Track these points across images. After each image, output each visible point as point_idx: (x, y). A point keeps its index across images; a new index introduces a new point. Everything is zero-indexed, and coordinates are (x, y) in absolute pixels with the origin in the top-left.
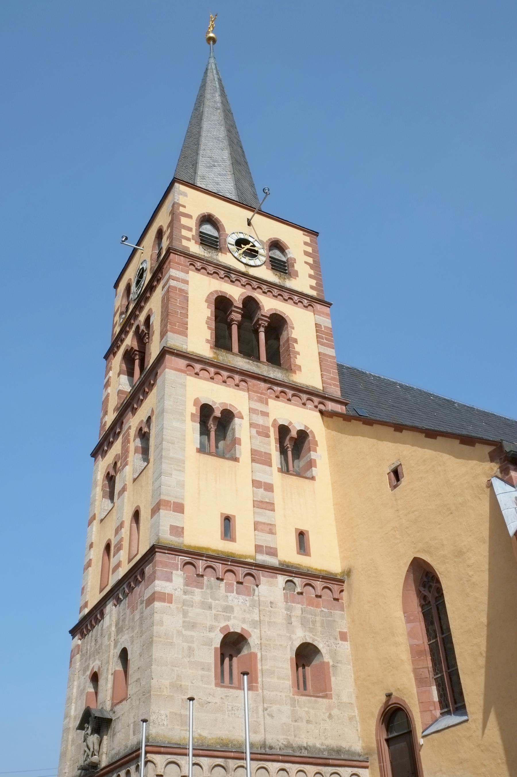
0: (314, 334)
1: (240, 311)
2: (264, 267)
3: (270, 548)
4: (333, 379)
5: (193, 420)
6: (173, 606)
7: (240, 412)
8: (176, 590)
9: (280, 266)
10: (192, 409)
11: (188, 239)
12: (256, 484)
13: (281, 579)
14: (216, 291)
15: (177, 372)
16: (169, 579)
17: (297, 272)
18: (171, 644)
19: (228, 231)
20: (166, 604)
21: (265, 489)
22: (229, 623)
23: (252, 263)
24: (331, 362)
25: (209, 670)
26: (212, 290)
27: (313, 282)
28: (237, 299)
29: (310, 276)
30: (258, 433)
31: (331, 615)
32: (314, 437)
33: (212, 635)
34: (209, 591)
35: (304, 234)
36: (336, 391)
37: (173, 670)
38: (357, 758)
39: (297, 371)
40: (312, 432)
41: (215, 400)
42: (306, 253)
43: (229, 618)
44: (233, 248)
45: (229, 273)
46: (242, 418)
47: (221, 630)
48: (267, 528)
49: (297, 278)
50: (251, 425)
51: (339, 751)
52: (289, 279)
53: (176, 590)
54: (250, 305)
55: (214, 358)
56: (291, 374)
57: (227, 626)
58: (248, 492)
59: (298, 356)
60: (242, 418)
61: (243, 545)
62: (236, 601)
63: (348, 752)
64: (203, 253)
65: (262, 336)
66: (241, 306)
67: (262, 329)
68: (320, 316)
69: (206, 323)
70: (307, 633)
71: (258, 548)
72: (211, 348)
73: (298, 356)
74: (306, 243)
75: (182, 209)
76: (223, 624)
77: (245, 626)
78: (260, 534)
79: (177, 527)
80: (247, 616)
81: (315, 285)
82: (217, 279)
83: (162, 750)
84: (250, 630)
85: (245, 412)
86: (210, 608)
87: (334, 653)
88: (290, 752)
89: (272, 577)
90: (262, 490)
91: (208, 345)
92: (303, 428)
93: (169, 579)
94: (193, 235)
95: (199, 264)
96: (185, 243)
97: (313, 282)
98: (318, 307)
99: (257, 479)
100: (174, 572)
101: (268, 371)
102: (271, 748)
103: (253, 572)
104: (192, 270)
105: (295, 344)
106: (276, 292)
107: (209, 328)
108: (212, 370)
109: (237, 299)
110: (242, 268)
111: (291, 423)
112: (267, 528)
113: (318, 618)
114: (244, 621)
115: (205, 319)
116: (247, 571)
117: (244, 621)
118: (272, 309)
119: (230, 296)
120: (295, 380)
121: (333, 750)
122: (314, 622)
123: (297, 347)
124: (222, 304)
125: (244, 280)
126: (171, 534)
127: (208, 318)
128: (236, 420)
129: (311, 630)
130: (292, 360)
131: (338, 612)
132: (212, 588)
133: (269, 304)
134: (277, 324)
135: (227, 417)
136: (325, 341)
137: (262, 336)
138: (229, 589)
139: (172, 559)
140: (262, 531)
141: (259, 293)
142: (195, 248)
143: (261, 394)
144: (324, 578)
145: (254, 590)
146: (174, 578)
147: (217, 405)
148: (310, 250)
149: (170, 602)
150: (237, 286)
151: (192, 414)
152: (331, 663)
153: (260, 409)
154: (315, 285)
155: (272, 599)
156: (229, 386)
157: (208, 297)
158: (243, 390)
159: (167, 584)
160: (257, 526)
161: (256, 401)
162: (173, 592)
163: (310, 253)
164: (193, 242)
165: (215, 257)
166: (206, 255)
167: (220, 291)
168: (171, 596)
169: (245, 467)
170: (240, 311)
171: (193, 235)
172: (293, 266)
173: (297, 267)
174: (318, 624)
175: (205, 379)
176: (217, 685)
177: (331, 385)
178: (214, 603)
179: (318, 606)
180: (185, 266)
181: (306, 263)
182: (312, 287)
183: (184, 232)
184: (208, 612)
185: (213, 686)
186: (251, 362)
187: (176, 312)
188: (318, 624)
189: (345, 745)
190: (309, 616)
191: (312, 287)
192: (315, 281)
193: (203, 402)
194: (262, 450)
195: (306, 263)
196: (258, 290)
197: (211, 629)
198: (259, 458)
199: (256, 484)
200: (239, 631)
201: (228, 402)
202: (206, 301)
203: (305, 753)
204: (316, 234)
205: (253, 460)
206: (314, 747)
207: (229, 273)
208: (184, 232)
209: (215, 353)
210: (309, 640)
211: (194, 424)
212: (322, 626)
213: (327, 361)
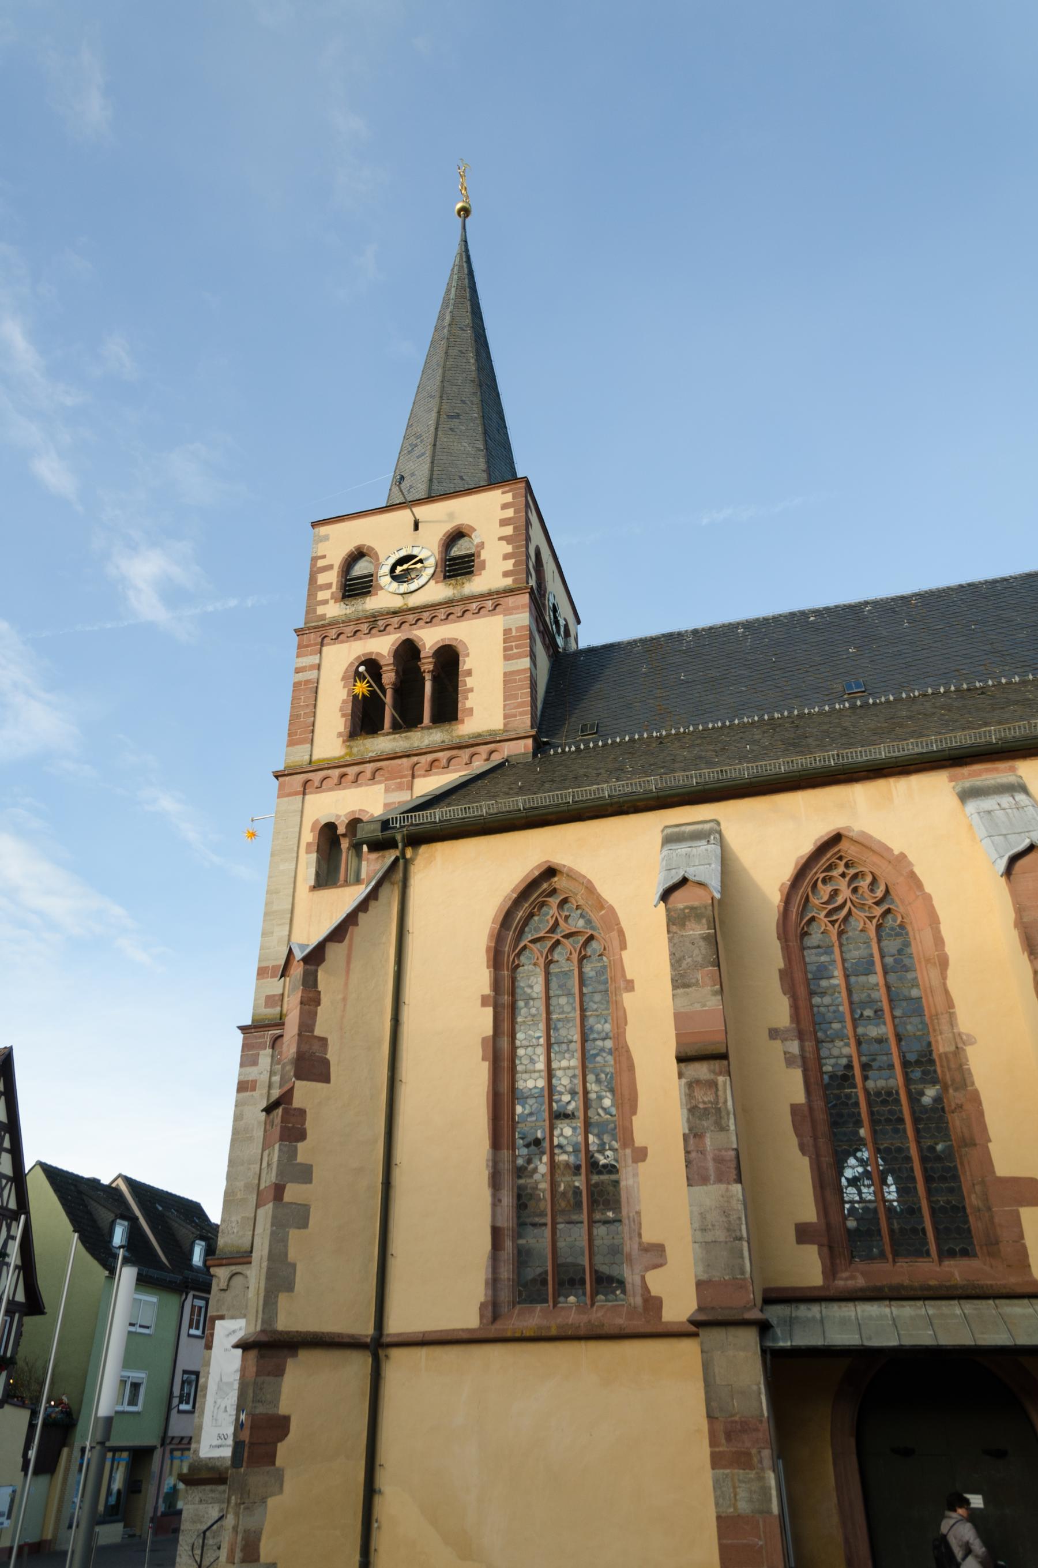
0: (501, 645)
2: (432, 582)
5: (308, 852)
6: (256, 1094)
8: (261, 1073)
9: (457, 565)
10: (309, 837)
11: (325, 602)
14: (359, 657)
15: (286, 799)
17: (484, 561)
18: (251, 1139)
19: (382, 559)
20: (248, 1093)
23: (413, 586)
24: (520, 680)
29: (506, 557)
35: (503, 493)
37: (249, 1169)
41: (339, 813)
44: (385, 580)
49: (483, 572)
52: (469, 580)
53: (261, 1073)
54: (408, 651)
55: (346, 754)
56: (455, 727)
59: (470, 695)
64: (344, 612)
65: (428, 686)
66: (391, 661)
67: (428, 677)
69: (341, 710)
72: (344, 742)
74: (505, 506)
75: (321, 563)
79: (274, 995)
82: (361, 639)
83: (224, 1262)
91: (341, 739)
93: (254, 1063)
94: (332, 593)
95: (334, 631)
96: (320, 610)
98: (511, 601)
100: (262, 1052)
101: (422, 737)
104: (329, 644)
105: (468, 679)
107: (343, 716)
108: (336, 772)
110: (397, 603)
115: (339, 704)
119: (378, 654)
120: (461, 733)
123: (469, 682)
125: (395, 620)
127: (344, 702)
130: (460, 705)
133: (430, 638)
134: (449, 658)
136: (515, 651)
137: (428, 686)
139: (260, 1037)
141: (421, 628)
142: (333, 610)
146: (260, 1060)
147: (343, 818)
148: (510, 513)
149: (254, 1089)
150: (389, 634)
151: (308, 844)
156: (360, 785)
158: (380, 782)
161: (393, 790)
163: (510, 519)
165: (360, 608)
166: (348, 612)
168: (254, 1082)
172: (479, 556)
173: (484, 555)
175: (330, 790)
177: (515, 716)
180: (316, 644)
181: (501, 539)
182: (506, 574)
186: (397, 736)
187: (298, 716)
191: (506, 574)
192: (513, 561)
193: (323, 822)
195: (501, 539)
196: (420, 623)
201: (356, 808)
202: (342, 680)
209: (350, 747)
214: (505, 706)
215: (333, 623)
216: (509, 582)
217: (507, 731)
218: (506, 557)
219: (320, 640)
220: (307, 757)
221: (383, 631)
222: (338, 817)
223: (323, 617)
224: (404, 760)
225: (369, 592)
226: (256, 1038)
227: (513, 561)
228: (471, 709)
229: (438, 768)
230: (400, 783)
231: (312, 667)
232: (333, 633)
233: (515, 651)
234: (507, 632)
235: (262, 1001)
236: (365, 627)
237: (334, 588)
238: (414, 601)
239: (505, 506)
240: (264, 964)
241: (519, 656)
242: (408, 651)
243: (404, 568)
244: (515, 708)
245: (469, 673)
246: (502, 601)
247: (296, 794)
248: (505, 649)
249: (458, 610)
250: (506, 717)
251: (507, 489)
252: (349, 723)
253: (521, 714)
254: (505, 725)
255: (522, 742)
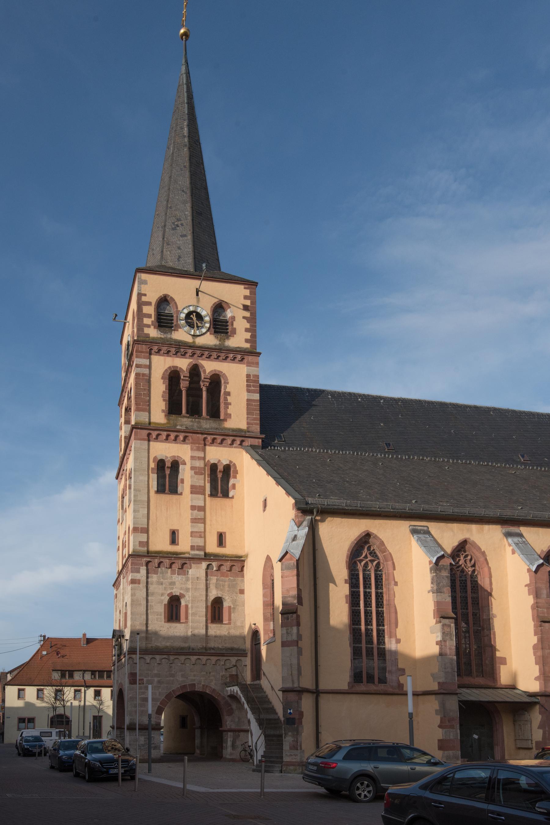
1: (187, 378)
3: (200, 546)
4: (255, 419)
6: (141, 585)
7: (184, 461)
9: (220, 326)
10: (152, 465)
12: (193, 508)
13: (204, 565)
14: (170, 368)
16: (138, 572)
18: (140, 604)
19: (180, 308)
21: (198, 511)
22: (173, 591)
23: (198, 333)
24: (255, 405)
25: (161, 615)
26: (167, 366)
27: (248, 335)
28: (185, 370)
29: (247, 330)
30: (196, 473)
31: (234, 580)
32: (235, 467)
33: (163, 598)
34: (161, 575)
35: (245, 288)
36: (256, 428)
38: (243, 653)
39: (228, 419)
40: (234, 464)
41: (167, 455)
42: (246, 308)
43: (172, 589)
45: (180, 349)
46: (185, 464)
47: (168, 595)
48: (198, 535)
50: (192, 468)
51: (232, 649)
52: (228, 338)
54: (195, 371)
55: (167, 423)
57: (172, 593)
58: (187, 514)
59: (229, 406)
60: (185, 464)
61: (184, 545)
62: (177, 579)
63: (238, 649)
64: (160, 336)
68: (250, 366)
70: (219, 592)
71: (193, 548)
72: (165, 416)
73: (229, 406)
74: (246, 297)
76: (169, 592)
77: (182, 592)
78: (194, 539)
79: (143, 542)
80: (184, 586)
81: (249, 338)
84: (184, 593)
85: (187, 459)
86: (162, 584)
87: (234, 602)
88: (204, 651)
89: (199, 564)
90: (196, 511)
91: (163, 414)
92: (228, 463)
93: (138, 572)
94: (152, 321)
97: (248, 335)
99: (193, 504)
102: (193, 649)
103: (187, 562)
106: (214, 355)
107: (164, 400)
108: (165, 433)
109: (185, 370)
110: (189, 339)
111: (219, 461)
112: (198, 535)
113: (226, 583)
114: (181, 589)
115: (161, 393)
116: (184, 562)
117: (181, 589)
118: (212, 371)
119: (180, 368)
121: (229, 649)
122: (223, 586)
124: (173, 377)
125: (190, 351)
126: (140, 546)
128: (181, 467)
129: (221, 590)
131: (240, 579)
132: (163, 573)
133: (209, 366)
134: (216, 381)
135: (175, 465)
136: (252, 388)
138: (173, 573)
140: (195, 537)
143: (199, 444)
144: (231, 560)
145: (188, 572)
146: (141, 571)
147: (169, 459)
148: (248, 303)
149: (139, 583)
152: (232, 606)
153: (197, 455)
154: (249, 338)
155: (198, 576)
157: (164, 374)
158: (187, 444)
159: (138, 574)
160: (193, 534)
161: (195, 450)
162: (140, 578)
163: (248, 306)
164: (152, 327)
166: (162, 336)
167: (173, 367)
169: (187, 498)
170: (187, 378)
171: (152, 321)
172: (232, 325)
173: (235, 325)
174: (226, 587)
176: (165, 622)
177: (252, 425)
178: (164, 581)
179: (227, 577)
180: (146, 352)
181: (244, 318)
182: (247, 341)
183: (147, 321)
184: (160, 586)
185: (163, 623)
187: (140, 394)
188: (226, 587)
189: (236, 646)
190: (221, 583)
191: (247, 341)
192: (250, 334)
193: (159, 458)
194: (198, 484)
195: (244, 318)
197: (162, 595)
198: (195, 490)
199: (193, 508)
200: (178, 594)
201: (176, 455)
202: (162, 378)
203: (213, 651)
204: (255, 284)
205: (191, 493)
206: (218, 648)
207: (180, 349)
208: (147, 321)
209: (168, 420)
210: (220, 596)
211: (154, 475)
212: (229, 587)
213: (252, 405)
214: (247, 417)
215: (153, 342)
216: (247, 345)
217: (248, 432)
218: (247, 330)
219: (148, 350)
220: (147, 420)
221: (184, 355)
222: (167, 457)
223: (147, 335)
224: (200, 435)
225: (172, 327)
226: (138, 560)
227: (250, 334)
228: (230, 415)
229: (216, 443)
230: (198, 447)
231: (145, 366)
232: (155, 348)
233: (252, 388)
234: (248, 376)
235: (137, 543)
236: (173, 350)
237: (153, 319)
238: (200, 341)
239: (246, 297)
240: (137, 526)
241: (254, 392)
242: (195, 371)
243: (193, 318)
244: (253, 420)
245: (229, 394)
246: (246, 357)
247: (144, 440)
248: (247, 386)
249: (223, 355)
250: (248, 423)
251: (246, 286)
252: (168, 404)
253: (256, 424)
254: (248, 428)
255: (257, 440)
